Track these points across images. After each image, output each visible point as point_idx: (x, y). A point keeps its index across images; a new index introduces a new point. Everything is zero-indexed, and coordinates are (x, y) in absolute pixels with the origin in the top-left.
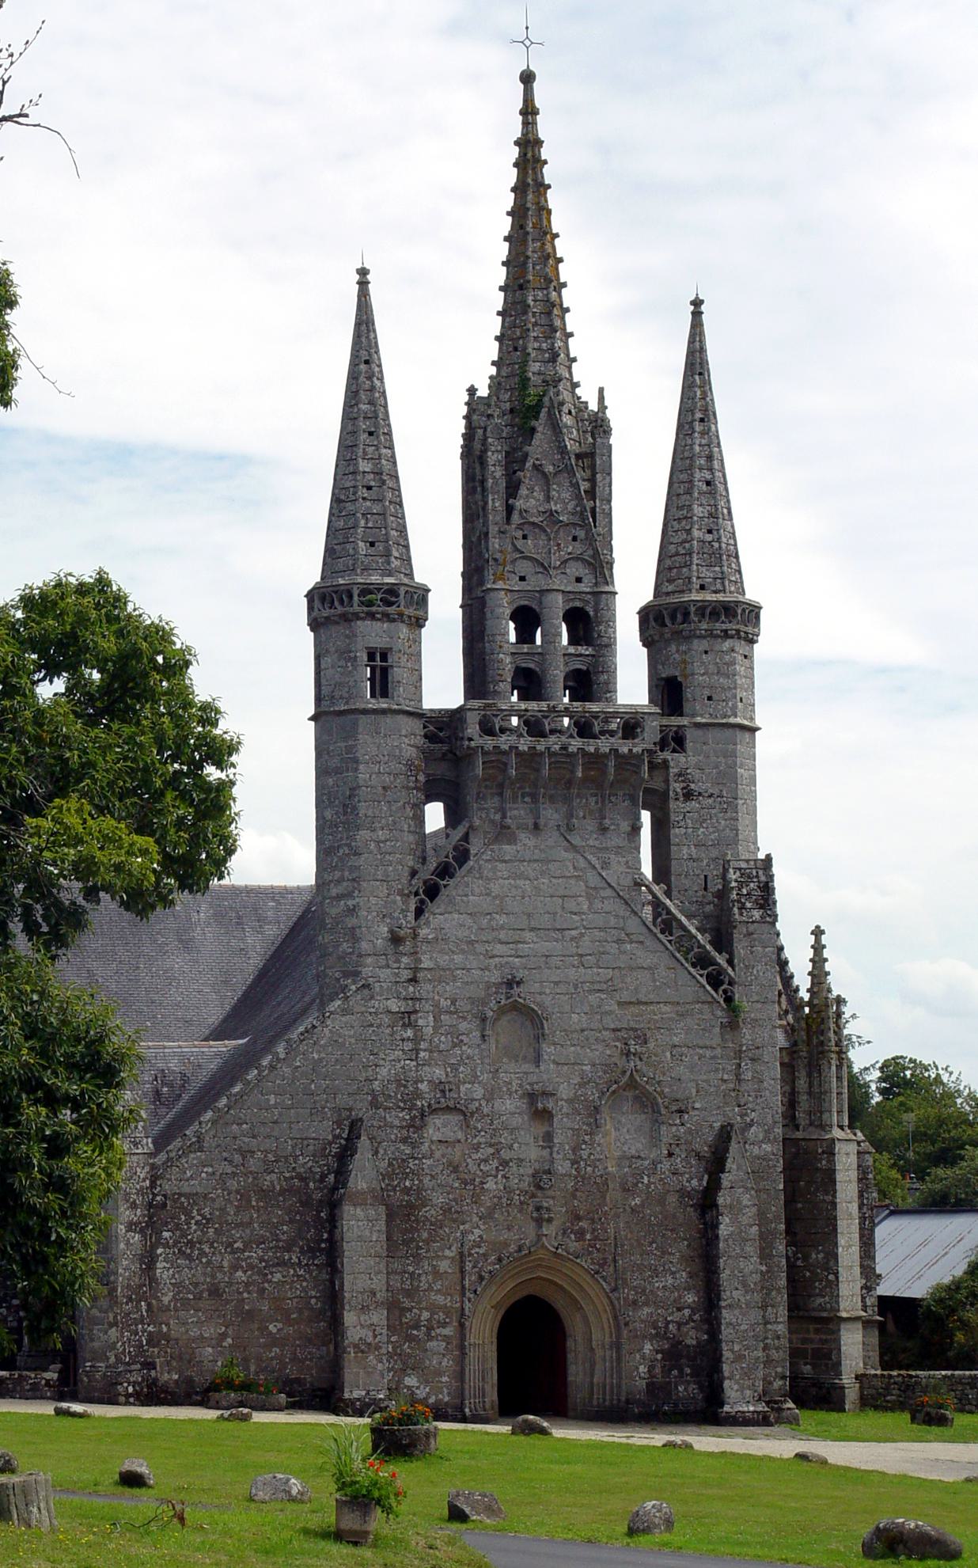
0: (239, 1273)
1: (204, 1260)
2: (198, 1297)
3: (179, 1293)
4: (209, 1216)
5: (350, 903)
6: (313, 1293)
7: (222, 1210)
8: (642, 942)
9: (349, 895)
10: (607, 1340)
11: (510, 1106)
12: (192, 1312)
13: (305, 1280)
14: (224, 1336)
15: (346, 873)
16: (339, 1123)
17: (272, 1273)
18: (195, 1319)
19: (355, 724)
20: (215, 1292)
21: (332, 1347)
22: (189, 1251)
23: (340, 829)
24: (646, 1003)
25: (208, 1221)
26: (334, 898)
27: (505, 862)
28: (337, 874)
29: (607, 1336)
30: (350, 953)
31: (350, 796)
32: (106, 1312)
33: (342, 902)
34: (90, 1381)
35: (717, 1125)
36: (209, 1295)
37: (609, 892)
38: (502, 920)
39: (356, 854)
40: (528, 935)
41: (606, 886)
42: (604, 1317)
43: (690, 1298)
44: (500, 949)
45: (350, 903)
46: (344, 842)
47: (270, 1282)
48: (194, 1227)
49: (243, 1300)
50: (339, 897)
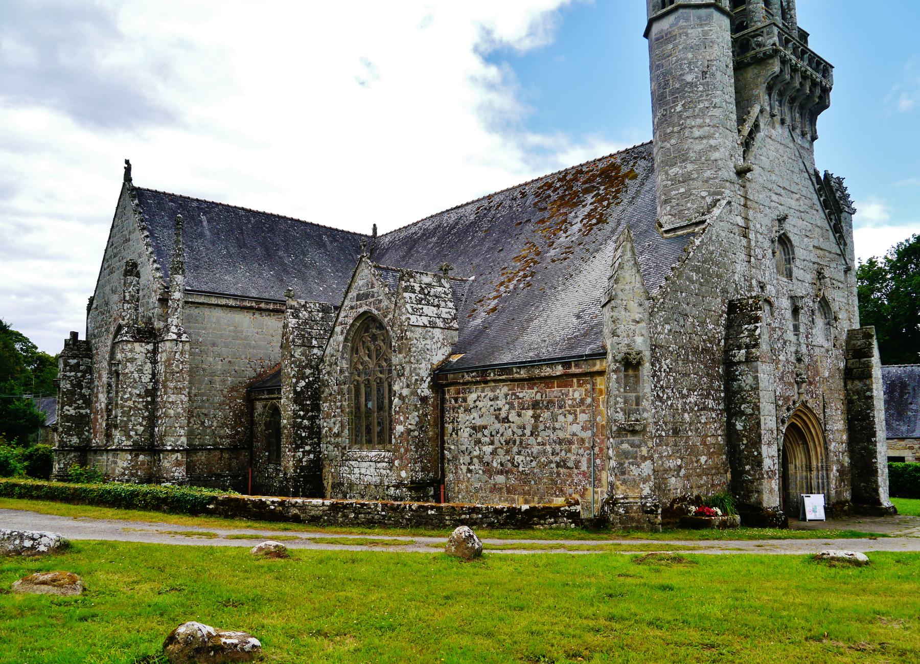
0: (686, 415)
1: (669, 403)
2: (667, 435)
3: (658, 430)
4: (670, 366)
5: (712, 142)
6: (719, 432)
7: (676, 361)
8: (817, 211)
9: (709, 136)
10: (820, 465)
11: (785, 303)
12: (664, 447)
13: (715, 422)
14: (680, 467)
15: (708, 121)
16: (723, 301)
17: (701, 415)
18: (666, 453)
19: (710, 17)
20: (676, 432)
21: (729, 475)
22: (661, 395)
23: (700, 89)
24: (821, 249)
25: (670, 369)
26: (697, 138)
27: (773, 140)
28: (699, 121)
29: (820, 461)
30: (714, 178)
31: (708, 66)
32: (639, 446)
33: (705, 141)
34: (627, 512)
35: (846, 330)
36: (673, 433)
37: (806, 175)
38: (774, 178)
39: (715, 107)
40: (783, 192)
41: (805, 170)
42: (819, 449)
43: (845, 437)
44: (774, 197)
45: (712, 142)
46: (704, 98)
47: (700, 422)
48: (664, 374)
49: (689, 437)
50: (701, 138)
